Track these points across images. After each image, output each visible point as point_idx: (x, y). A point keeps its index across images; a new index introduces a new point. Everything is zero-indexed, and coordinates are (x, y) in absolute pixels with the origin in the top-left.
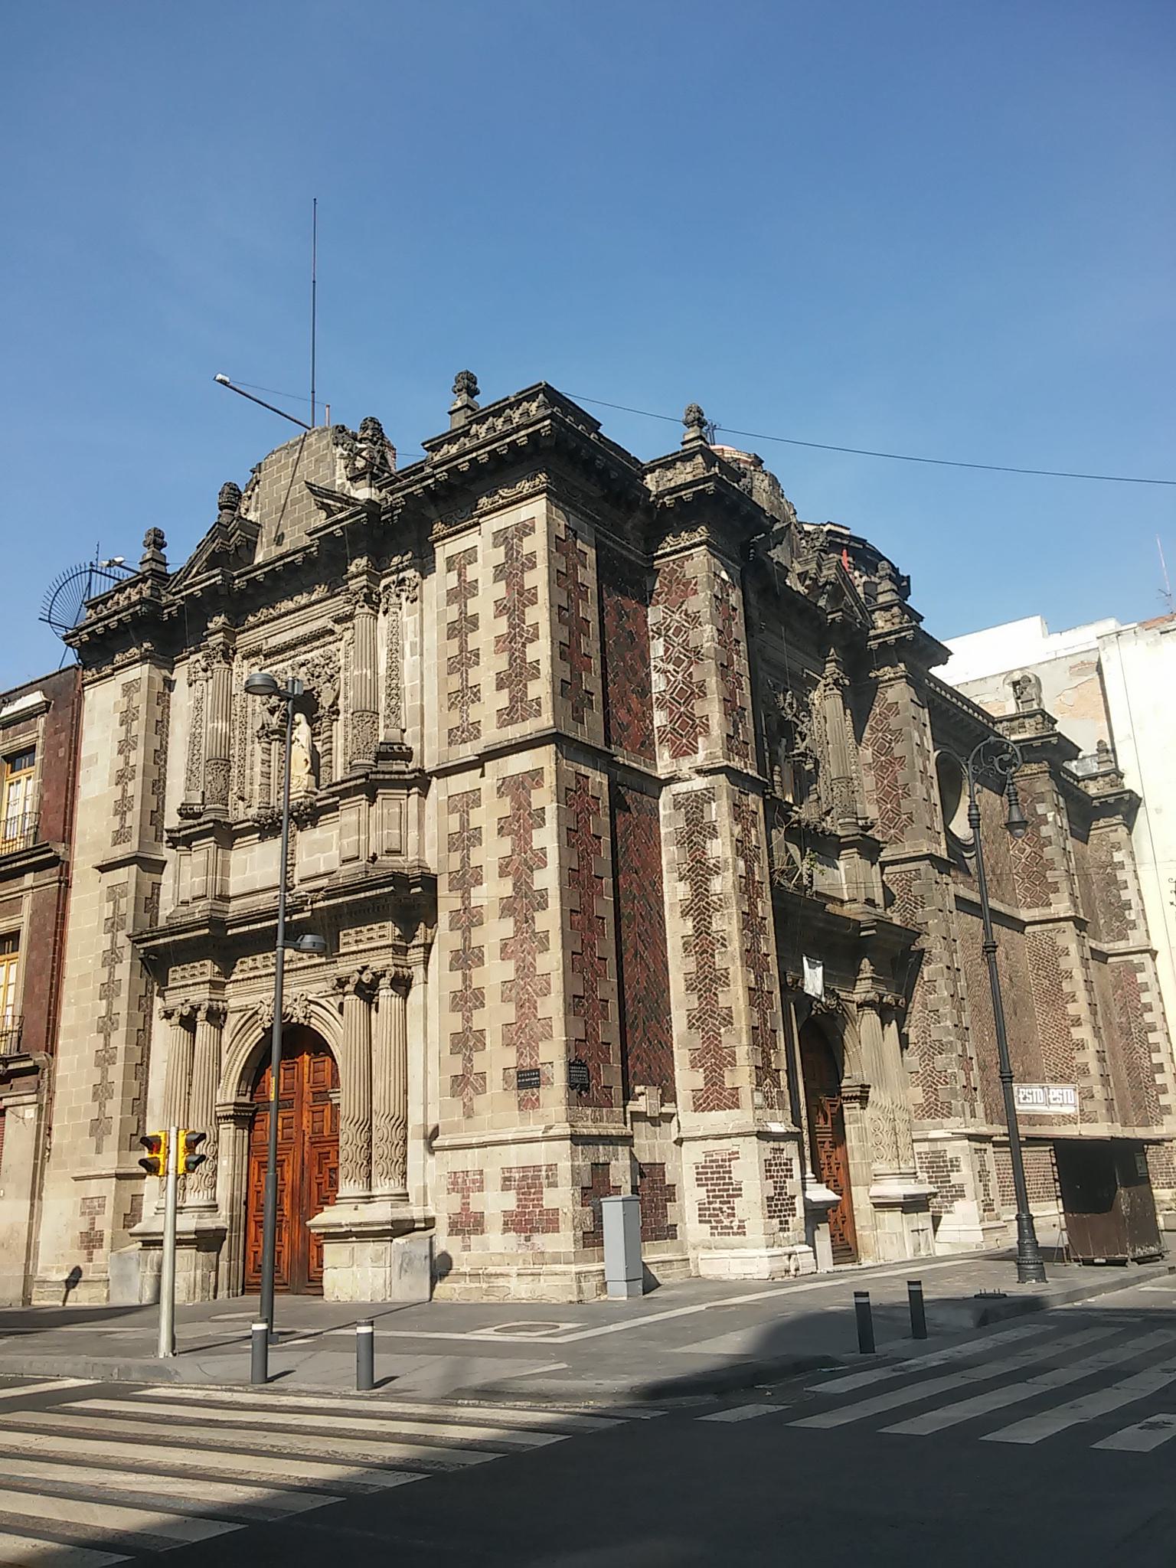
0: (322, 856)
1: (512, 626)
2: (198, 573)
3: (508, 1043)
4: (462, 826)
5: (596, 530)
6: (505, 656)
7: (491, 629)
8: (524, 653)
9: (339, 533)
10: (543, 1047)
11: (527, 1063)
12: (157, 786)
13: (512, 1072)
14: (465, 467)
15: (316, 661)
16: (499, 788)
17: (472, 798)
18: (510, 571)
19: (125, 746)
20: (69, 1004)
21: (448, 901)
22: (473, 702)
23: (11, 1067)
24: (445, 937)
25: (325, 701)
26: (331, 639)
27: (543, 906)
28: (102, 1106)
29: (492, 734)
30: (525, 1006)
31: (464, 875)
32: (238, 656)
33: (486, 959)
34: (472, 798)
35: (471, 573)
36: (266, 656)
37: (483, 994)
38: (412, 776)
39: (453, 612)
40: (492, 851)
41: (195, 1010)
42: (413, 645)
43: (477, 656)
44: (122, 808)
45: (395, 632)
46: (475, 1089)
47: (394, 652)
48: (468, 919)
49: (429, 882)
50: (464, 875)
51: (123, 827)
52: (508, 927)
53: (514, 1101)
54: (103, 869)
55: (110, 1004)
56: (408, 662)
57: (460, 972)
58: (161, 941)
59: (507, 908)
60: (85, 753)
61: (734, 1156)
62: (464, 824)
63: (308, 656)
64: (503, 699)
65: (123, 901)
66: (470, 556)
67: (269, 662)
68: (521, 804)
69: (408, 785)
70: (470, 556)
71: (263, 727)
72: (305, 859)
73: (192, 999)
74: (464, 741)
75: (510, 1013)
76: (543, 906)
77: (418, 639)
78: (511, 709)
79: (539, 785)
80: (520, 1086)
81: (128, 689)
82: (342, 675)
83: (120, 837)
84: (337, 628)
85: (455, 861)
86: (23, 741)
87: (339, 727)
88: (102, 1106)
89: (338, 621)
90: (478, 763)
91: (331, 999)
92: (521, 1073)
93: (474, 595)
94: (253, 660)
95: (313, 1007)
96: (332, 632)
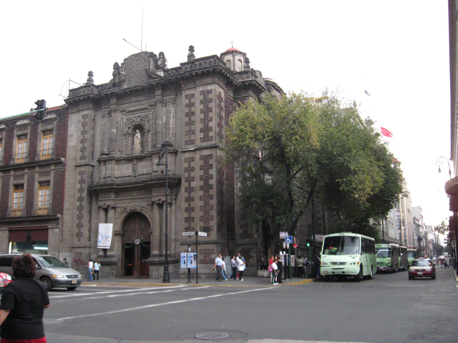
1: (205, 116)
2: (109, 88)
3: (201, 220)
4: (189, 166)
5: (225, 92)
6: (203, 124)
7: (198, 116)
8: (208, 124)
9: (154, 84)
11: (206, 225)
12: (93, 145)
13: (203, 228)
14: (194, 74)
15: (143, 116)
16: (200, 158)
17: (192, 159)
18: (206, 102)
19: (84, 133)
21: (184, 184)
22: (192, 134)
23: (51, 218)
24: (183, 193)
25: (146, 127)
26: (148, 111)
27: (212, 188)
28: (80, 229)
29: (199, 144)
30: (206, 213)
31: (189, 179)
32: (118, 112)
33: (195, 200)
34: (192, 159)
35: (193, 100)
36: (127, 113)
37: (194, 209)
38: (174, 151)
39: (187, 110)
40: (198, 173)
41: (108, 206)
42: (173, 116)
43: (194, 122)
44: (83, 150)
45: (168, 112)
47: (168, 118)
48: (190, 190)
49: (180, 180)
50: (189, 179)
51: (83, 155)
52: (202, 193)
54: (77, 166)
55: (81, 204)
56: (172, 120)
58: (99, 188)
59: (202, 188)
60: (69, 133)
61: (250, 249)
62: (189, 166)
63: (141, 114)
64: (202, 135)
65: (84, 176)
66: (193, 96)
67: (128, 114)
68: (206, 163)
69: (172, 153)
70: (193, 96)
71: (127, 132)
73: (107, 204)
74: (190, 144)
75: (202, 213)
76: (212, 188)
77: (175, 115)
78: (204, 138)
79: (212, 158)
81: (84, 117)
82: (151, 121)
83: (83, 158)
84: (150, 108)
85: (186, 175)
86: (49, 127)
87: (150, 135)
88: (80, 229)
89: (150, 106)
90: (195, 150)
91: (148, 207)
93: (193, 106)
94: (123, 113)
95: (142, 208)
96: (148, 109)
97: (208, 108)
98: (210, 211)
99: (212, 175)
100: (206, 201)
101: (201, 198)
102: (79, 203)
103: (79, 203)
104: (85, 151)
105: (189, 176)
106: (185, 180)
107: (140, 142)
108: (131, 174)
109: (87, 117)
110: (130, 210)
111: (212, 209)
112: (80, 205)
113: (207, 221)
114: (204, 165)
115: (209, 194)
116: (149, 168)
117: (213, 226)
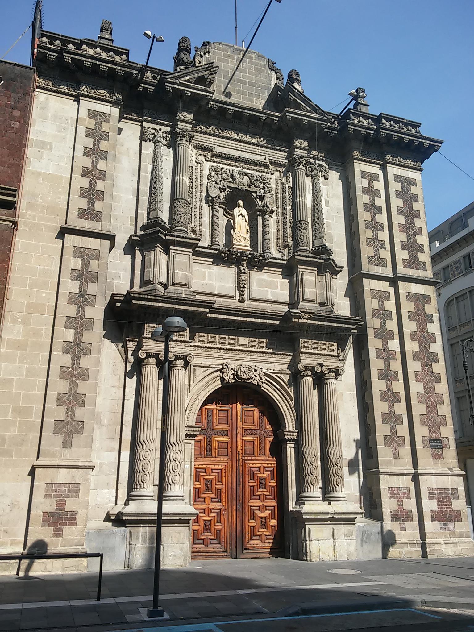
0: (270, 291)
9: (305, 122)
10: (442, 428)
20: (14, 321)
28: (70, 411)
46: (398, 444)
51: (89, 208)
53: (430, 454)
57: (384, 381)
72: (256, 288)
80: (431, 447)
91: (282, 376)
92: (430, 440)
94: (202, 153)
97: (411, 208)
98: (438, 406)
99: (433, 334)
100: (427, 384)
101: (416, 375)
102: (72, 332)
103: (72, 332)
104: (98, 200)
105: (381, 328)
106: (375, 333)
107: (248, 228)
108: (232, 293)
109: (108, 121)
110: (236, 376)
111: (442, 402)
112: (75, 340)
113: (433, 426)
114: (416, 313)
115: (432, 372)
116: (278, 290)
117: (447, 438)
